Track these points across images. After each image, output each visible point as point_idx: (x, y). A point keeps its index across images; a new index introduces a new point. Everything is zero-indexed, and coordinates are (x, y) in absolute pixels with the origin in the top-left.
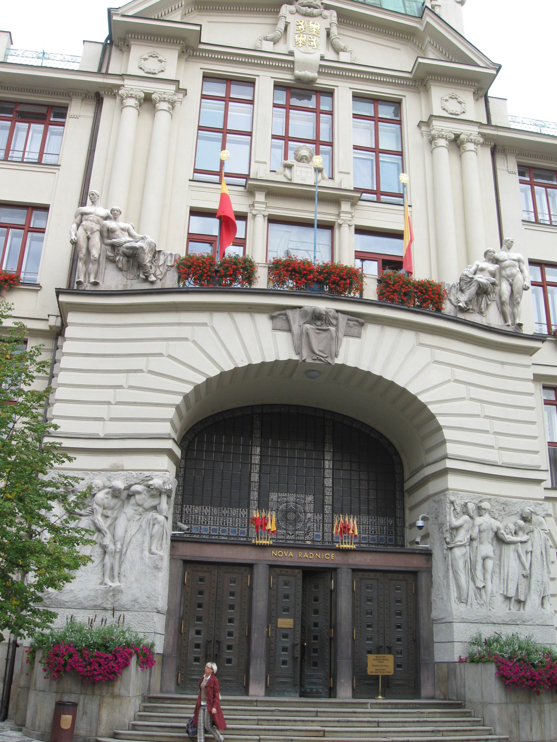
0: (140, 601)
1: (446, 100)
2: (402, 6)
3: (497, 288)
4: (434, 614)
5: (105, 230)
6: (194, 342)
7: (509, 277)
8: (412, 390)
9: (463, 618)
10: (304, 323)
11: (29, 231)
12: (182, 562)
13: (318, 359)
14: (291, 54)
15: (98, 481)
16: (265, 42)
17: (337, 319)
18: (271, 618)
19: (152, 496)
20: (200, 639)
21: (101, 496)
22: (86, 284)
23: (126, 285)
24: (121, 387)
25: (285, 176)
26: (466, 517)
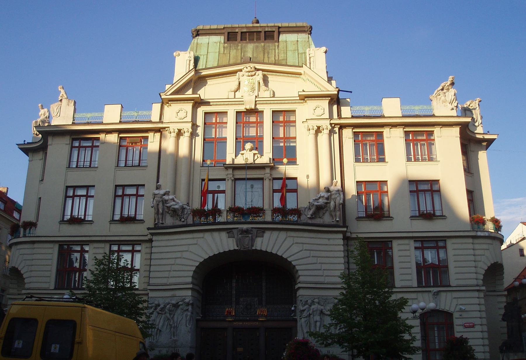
2: (297, 58)
5: (164, 200)
7: (334, 199)
8: (285, 256)
10: (239, 234)
17: (252, 231)
21: (168, 306)
23: (173, 223)
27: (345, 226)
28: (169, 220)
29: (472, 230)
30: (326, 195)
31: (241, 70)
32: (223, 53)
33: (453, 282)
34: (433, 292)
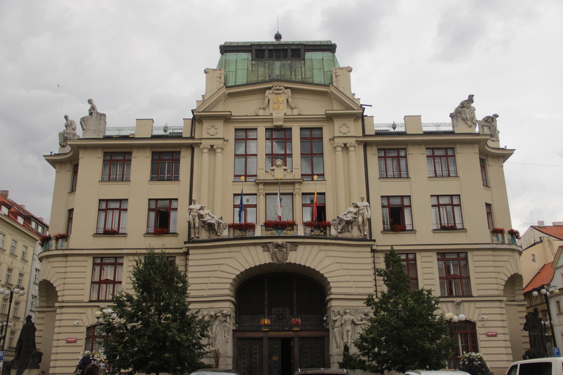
4: (330, 353)
6: (235, 258)
8: (317, 269)
13: (280, 262)
14: (272, 114)
16: (260, 110)
17: (287, 245)
18: (270, 357)
19: (224, 317)
22: (195, 238)
24: (210, 277)
26: (339, 316)
27: (371, 240)
28: (204, 235)
29: (492, 243)
30: (355, 210)
31: (269, 88)
32: (251, 70)
33: (474, 293)
34: (456, 302)
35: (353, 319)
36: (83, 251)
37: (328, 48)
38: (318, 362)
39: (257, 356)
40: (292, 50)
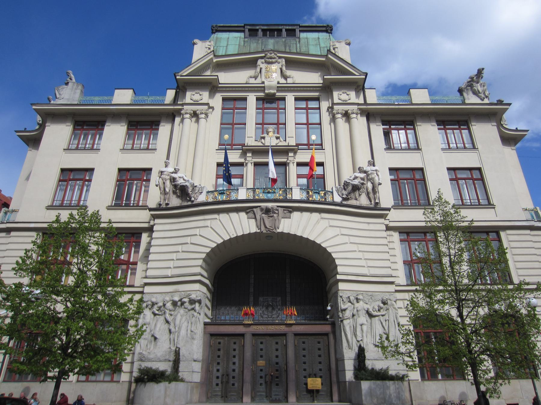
0: (186, 356)
1: (341, 95)
3: (365, 186)
7: (371, 179)
8: (318, 241)
9: (349, 357)
11: (143, 181)
12: (209, 335)
14: (263, 83)
15: (167, 298)
16: (251, 79)
17: (278, 210)
20: (219, 374)
24: (178, 252)
25: (262, 143)
26: (350, 304)
28: (175, 201)
31: (262, 58)
35: (368, 309)
36: (30, 224)
37: (324, 29)
38: (320, 370)
39: (236, 360)
40: (286, 30)
